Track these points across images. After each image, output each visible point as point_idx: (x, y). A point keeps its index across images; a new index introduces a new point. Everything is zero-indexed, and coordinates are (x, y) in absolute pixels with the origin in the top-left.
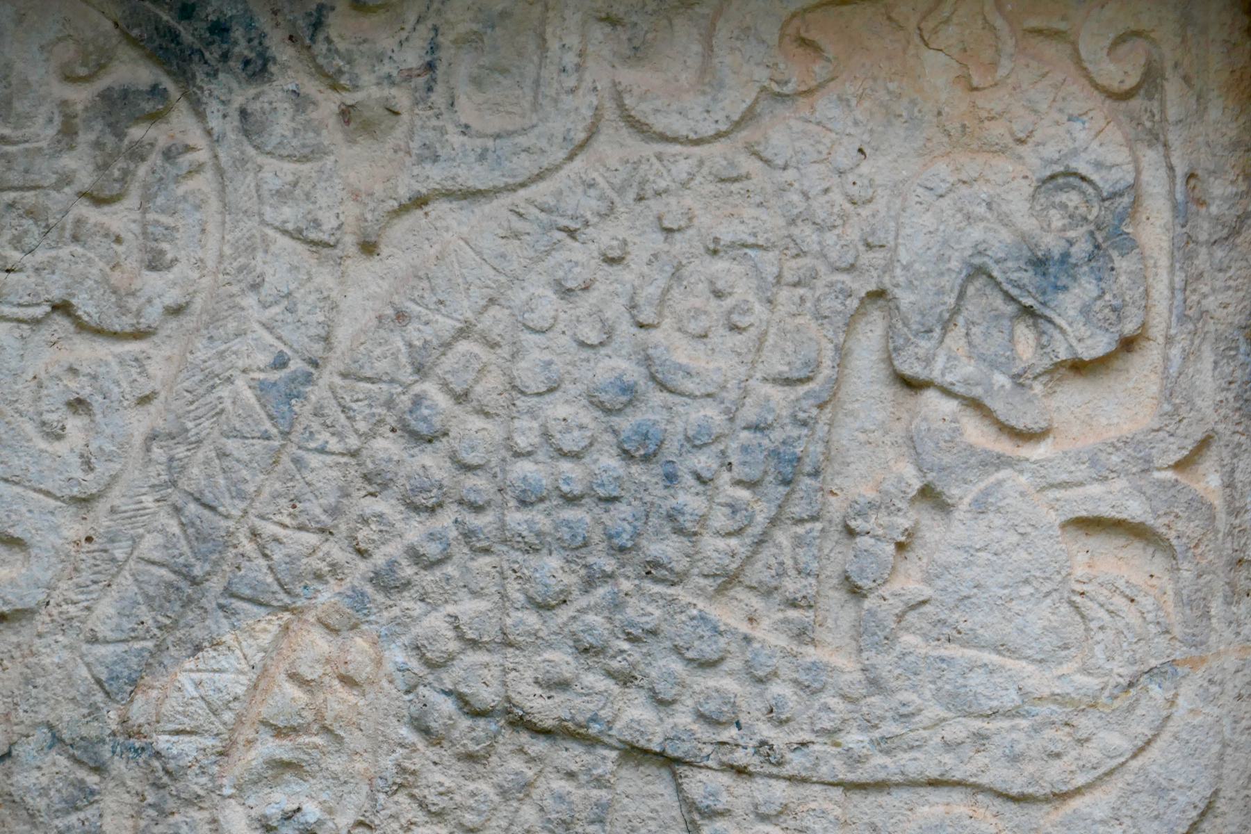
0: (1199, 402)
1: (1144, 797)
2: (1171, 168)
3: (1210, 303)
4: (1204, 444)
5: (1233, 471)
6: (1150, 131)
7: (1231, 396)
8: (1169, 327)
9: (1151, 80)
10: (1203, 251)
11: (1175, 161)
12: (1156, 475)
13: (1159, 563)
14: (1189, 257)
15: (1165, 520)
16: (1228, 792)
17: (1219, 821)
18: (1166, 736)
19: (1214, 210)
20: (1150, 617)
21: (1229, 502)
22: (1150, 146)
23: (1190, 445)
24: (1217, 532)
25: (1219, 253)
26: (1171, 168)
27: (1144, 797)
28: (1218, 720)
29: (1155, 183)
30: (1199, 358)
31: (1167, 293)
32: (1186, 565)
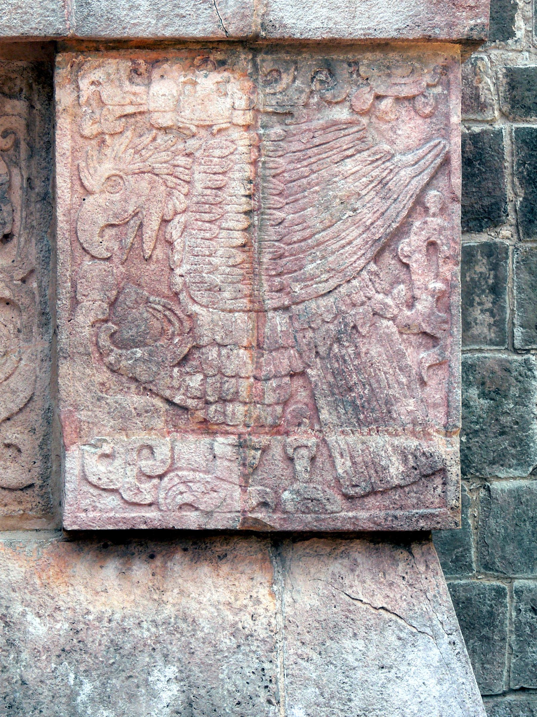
0: (30, 257)
1: (8, 394)
2: (22, 176)
3: (34, 223)
4: (32, 271)
5: (41, 282)
6: (15, 163)
7: (41, 255)
8: (20, 231)
9: (16, 144)
10: (33, 205)
11: (23, 173)
12: (15, 282)
13: (15, 313)
14: (27, 206)
15: (16, 298)
16: (37, 393)
17: (34, 403)
18: (16, 373)
19: (37, 190)
20: (12, 332)
21: (40, 292)
22: (15, 167)
23: (27, 271)
24: (35, 302)
25: (38, 206)
26: (22, 176)
27: (8, 394)
28: (35, 368)
29: (17, 181)
30: (31, 242)
31: (20, 219)
32: (24, 314)
